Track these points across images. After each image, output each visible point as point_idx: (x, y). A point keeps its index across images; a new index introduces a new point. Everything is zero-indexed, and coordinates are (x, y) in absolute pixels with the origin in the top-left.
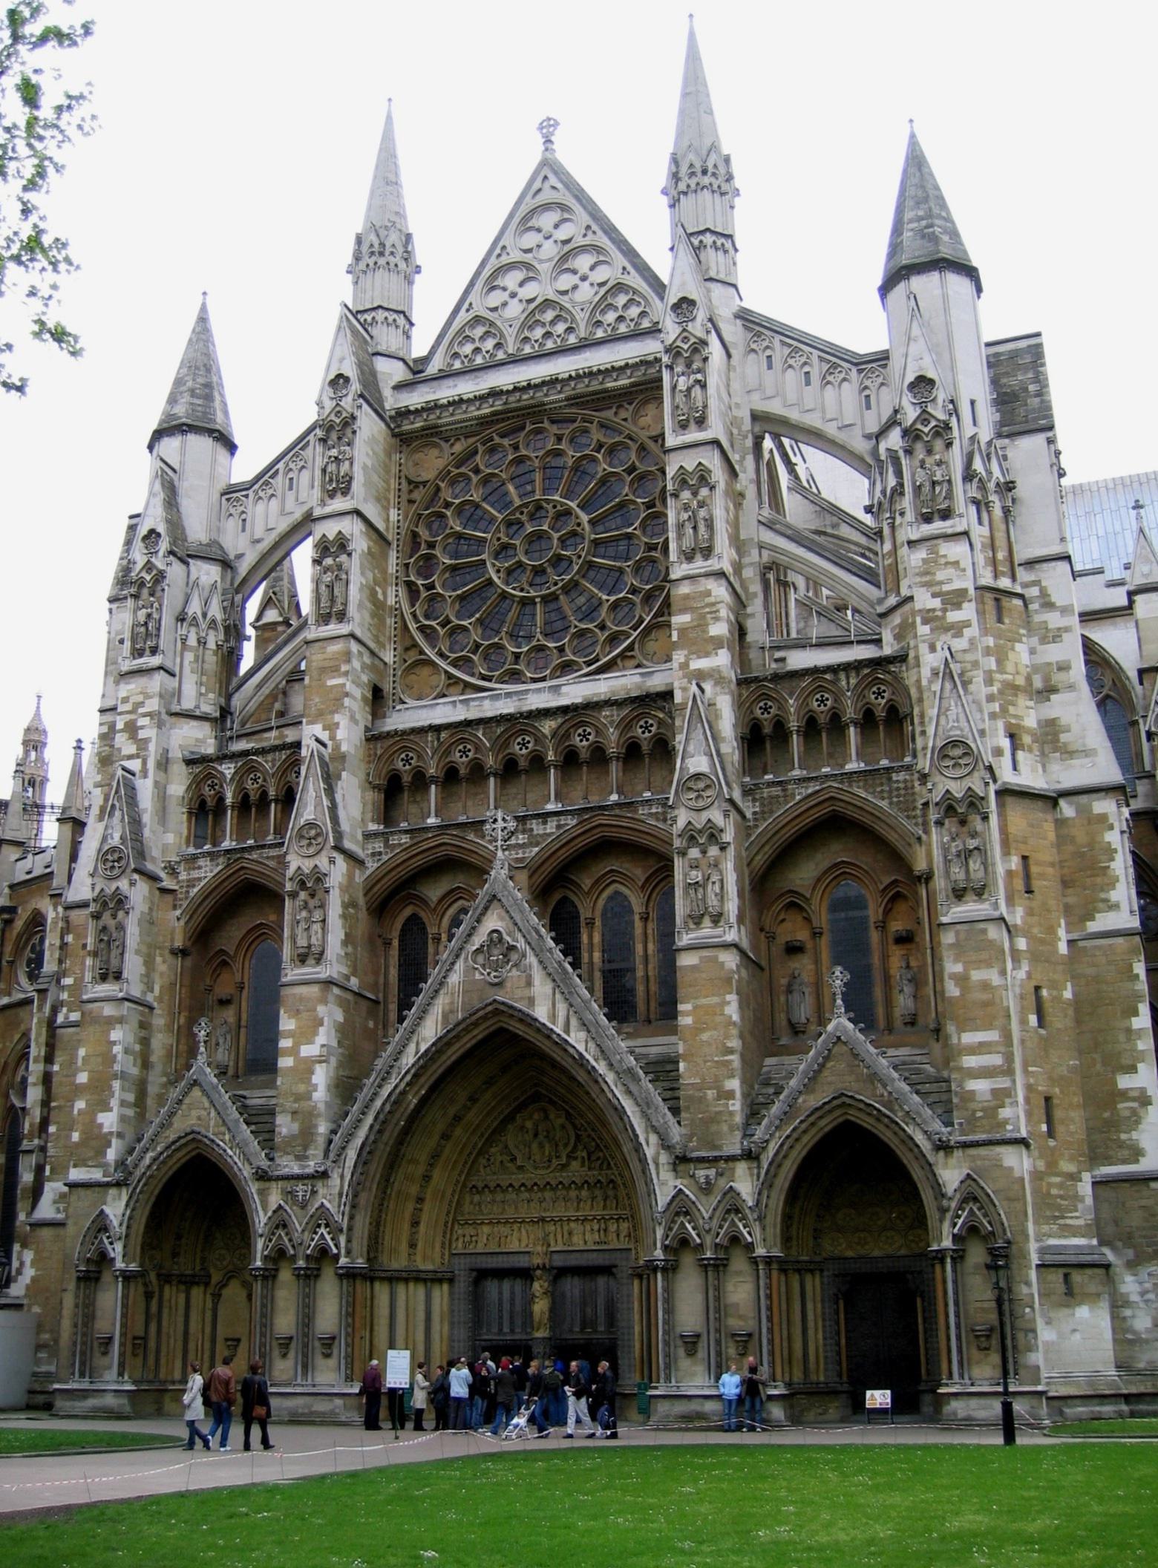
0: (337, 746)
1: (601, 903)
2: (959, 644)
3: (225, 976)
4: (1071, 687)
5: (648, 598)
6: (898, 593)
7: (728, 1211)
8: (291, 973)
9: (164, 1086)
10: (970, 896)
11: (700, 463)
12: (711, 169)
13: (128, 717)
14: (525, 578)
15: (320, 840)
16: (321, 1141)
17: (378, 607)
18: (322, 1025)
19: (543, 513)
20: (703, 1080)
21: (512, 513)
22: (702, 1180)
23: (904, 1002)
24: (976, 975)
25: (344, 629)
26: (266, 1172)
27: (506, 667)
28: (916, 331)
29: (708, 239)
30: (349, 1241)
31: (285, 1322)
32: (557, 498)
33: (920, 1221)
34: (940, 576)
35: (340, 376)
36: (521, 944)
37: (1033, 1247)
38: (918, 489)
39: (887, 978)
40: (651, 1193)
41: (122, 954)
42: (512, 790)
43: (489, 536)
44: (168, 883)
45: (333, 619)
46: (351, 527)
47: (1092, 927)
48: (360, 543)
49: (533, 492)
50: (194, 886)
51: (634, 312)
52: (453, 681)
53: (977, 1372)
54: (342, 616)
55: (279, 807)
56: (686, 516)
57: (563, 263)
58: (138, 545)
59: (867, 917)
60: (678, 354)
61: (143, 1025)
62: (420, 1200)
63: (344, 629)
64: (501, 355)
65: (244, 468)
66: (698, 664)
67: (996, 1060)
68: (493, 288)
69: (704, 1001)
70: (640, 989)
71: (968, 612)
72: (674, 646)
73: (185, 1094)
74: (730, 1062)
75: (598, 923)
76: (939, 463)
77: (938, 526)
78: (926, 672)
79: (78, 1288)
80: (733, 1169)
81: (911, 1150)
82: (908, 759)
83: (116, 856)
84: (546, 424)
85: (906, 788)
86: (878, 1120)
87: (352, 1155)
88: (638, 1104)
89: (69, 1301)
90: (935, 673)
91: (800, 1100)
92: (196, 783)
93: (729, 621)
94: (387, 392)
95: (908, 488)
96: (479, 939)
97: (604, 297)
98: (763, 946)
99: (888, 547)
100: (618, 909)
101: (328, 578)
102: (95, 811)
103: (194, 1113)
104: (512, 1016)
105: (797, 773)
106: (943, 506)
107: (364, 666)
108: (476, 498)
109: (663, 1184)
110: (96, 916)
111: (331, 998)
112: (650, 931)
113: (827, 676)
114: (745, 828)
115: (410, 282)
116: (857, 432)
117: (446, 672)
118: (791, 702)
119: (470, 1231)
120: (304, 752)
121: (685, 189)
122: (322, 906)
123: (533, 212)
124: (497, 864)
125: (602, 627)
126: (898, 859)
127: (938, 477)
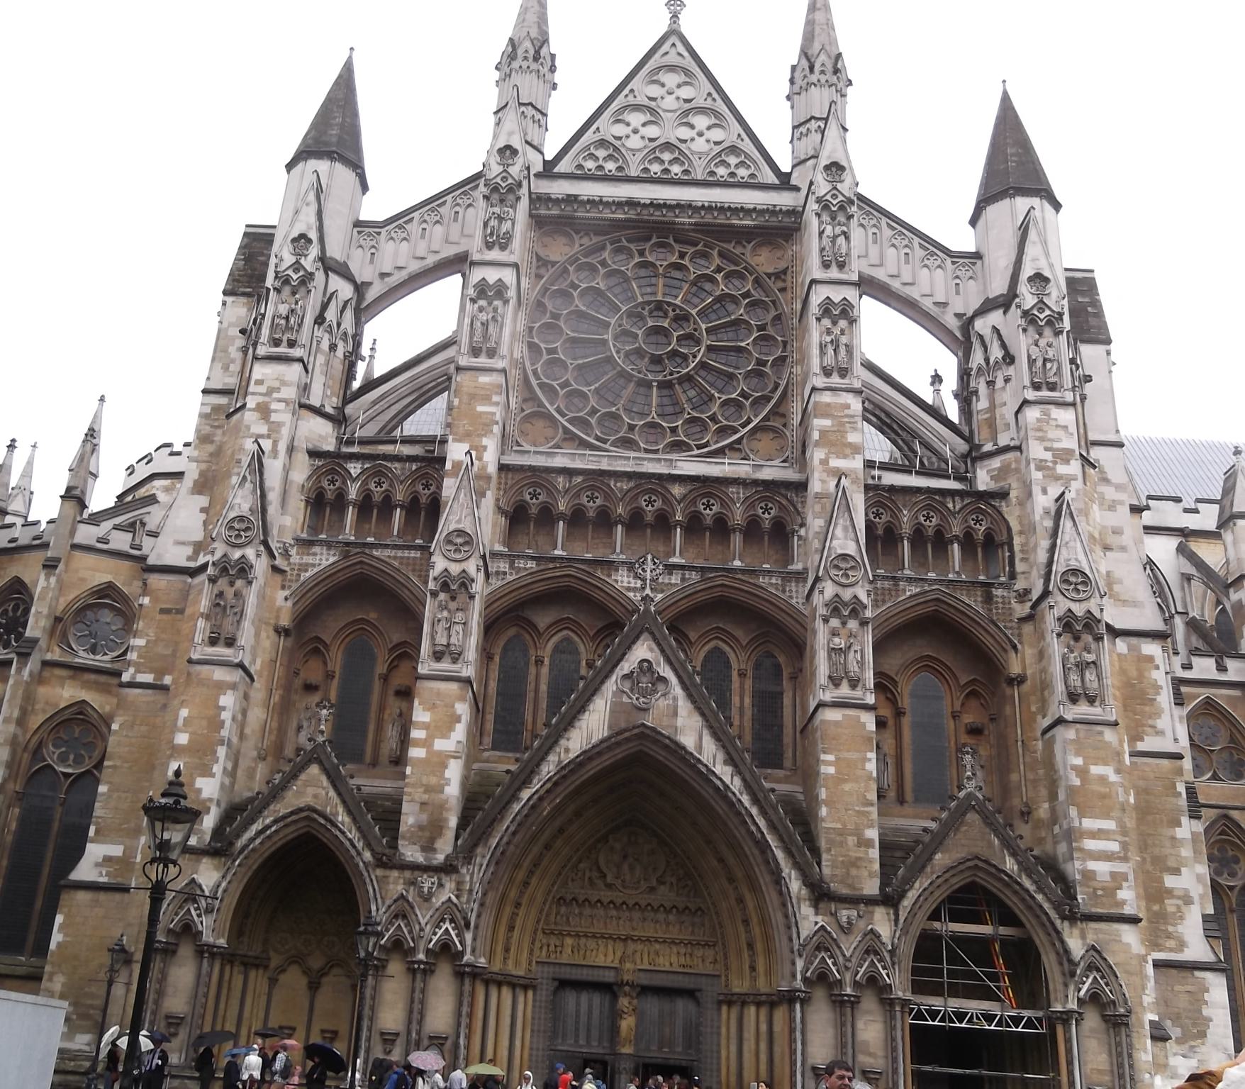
0: (484, 468)
1: (702, 655)
7: (867, 952)
8: (426, 666)
11: (845, 299)
18: (459, 721)
19: (661, 314)
22: (844, 919)
25: (500, 364)
27: (621, 434)
32: (678, 302)
35: (508, 147)
40: (790, 923)
45: (484, 354)
48: (512, 293)
49: (654, 294)
52: (570, 437)
54: (492, 353)
55: (404, 512)
56: (828, 339)
60: (826, 207)
65: (375, 208)
66: (835, 463)
68: (618, 121)
72: (817, 444)
80: (872, 913)
81: (1038, 917)
86: (1007, 885)
88: (781, 839)
91: (938, 856)
92: (316, 474)
97: (719, 154)
101: (483, 317)
104: (656, 742)
105: (907, 572)
108: (602, 286)
109: (806, 918)
112: (746, 687)
113: (937, 497)
117: (564, 427)
118: (905, 512)
120: (448, 466)
121: (815, 81)
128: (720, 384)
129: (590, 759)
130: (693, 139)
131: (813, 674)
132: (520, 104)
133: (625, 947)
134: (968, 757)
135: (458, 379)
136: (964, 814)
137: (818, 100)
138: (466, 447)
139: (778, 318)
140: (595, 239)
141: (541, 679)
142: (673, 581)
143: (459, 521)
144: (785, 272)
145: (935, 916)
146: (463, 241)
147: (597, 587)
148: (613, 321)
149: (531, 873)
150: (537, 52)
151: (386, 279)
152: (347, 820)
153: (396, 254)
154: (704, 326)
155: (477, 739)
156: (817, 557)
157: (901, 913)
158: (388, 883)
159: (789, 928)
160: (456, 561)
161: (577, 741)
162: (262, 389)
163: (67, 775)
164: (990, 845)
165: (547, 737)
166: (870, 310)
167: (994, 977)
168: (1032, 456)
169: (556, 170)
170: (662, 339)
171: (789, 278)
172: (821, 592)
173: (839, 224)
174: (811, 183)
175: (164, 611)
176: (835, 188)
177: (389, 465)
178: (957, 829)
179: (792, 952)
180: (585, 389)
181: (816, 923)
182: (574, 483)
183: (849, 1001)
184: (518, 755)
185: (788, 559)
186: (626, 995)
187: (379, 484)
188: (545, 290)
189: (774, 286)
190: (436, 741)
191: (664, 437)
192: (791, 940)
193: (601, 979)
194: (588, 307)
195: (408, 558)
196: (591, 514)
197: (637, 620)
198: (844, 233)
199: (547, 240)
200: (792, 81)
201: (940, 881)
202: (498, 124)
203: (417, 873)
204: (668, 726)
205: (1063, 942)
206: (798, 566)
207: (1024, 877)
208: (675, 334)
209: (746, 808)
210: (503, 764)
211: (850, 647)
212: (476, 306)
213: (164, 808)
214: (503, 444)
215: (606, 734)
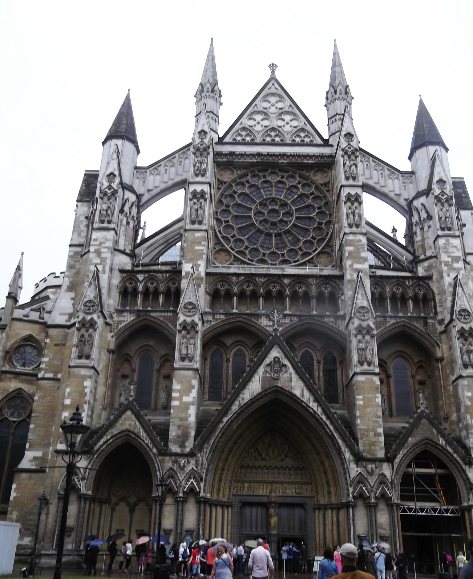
0: (200, 274)
3: (126, 365)
6: (425, 255)
7: (381, 483)
9: (101, 410)
14: (268, 226)
15: (193, 310)
16: (192, 439)
18: (193, 387)
19: (274, 203)
20: (368, 428)
21: (263, 200)
22: (370, 469)
25: (205, 227)
26: (165, 451)
27: (260, 257)
30: (205, 486)
31: (168, 523)
32: (282, 198)
34: (451, 250)
35: (203, 131)
38: (440, 218)
40: (346, 472)
41: (91, 348)
43: (253, 207)
44: (108, 320)
49: (271, 194)
50: (121, 324)
52: (236, 260)
54: (200, 223)
56: (350, 211)
60: (346, 153)
61: (96, 382)
65: (143, 161)
66: (356, 266)
68: (250, 119)
69: (367, 395)
72: (348, 258)
73: (124, 412)
74: (379, 421)
76: (447, 211)
77: (446, 232)
78: (446, 284)
79: (59, 503)
80: (382, 465)
81: (455, 464)
83: (91, 304)
84: (277, 171)
85: (432, 325)
86: (441, 450)
90: (450, 284)
91: (410, 439)
92: (123, 280)
97: (296, 132)
101: (196, 207)
103: (127, 422)
105: (390, 314)
106: (449, 226)
108: (248, 192)
109: (353, 469)
112: (321, 368)
117: (234, 255)
118: (387, 287)
120: (183, 274)
123: (268, 95)
127: (448, 214)
128: (302, 233)
129: (254, 402)
130: (284, 126)
131: (351, 360)
132: (208, 112)
133: (272, 486)
134: (421, 395)
135: (186, 235)
136: (421, 420)
137: (339, 106)
138: (191, 265)
139: (326, 204)
140: (243, 171)
141: (229, 368)
142: (286, 322)
143: (190, 298)
144: (328, 183)
145: (409, 466)
146: (184, 174)
147: (253, 326)
148: (253, 207)
149: (228, 455)
151: (151, 192)
152: (145, 435)
153: (154, 181)
154: (294, 208)
156: (350, 308)
157: (395, 465)
158: (165, 463)
159: (345, 474)
160: (189, 316)
161: (247, 395)
162: (97, 243)
163: (14, 422)
164: (433, 433)
165: (234, 394)
166: (366, 197)
167: (436, 492)
168: (442, 260)
169: (224, 141)
170: (275, 215)
171: (330, 186)
172: (353, 323)
173: (352, 160)
174: (339, 142)
175: (56, 345)
176: (349, 144)
177: (156, 275)
178: (418, 427)
179: (347, 484)
180: (242, 238)
181: (357, 471)
182: (240, 279)
183: (373, 505)
184: (220, 402)
185: (337, 310)
186: (273, 507)
187: (152, 284)
188: (222, 195)
189: (324, 189)
191: (279, 258)
192: (346, 479)
193: (261, 501)
194: (242, 201)
195: (167, 316)
196: (248, 293)
197: (271, 339)
198: (355, 164)
199: (222, 172)
200: (327, 98)
201: (411, 450)
202: (197, 121)
203: (177, 457)
204: (288, 386)
205: (466, 475)
206: (341, 313)
207: (448, 447)
208: (281, 212)
209: (324, 422)
210: (214, 407)
211: (367, 348)
212: (192, 202)
213: (71, 426)
214: (207, 263)
215: (260, 391)
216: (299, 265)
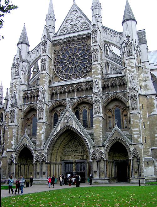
1: (82, 111)
2: (133, 74)
3: (29, 122)
4: (149, 80)
5: (89, 67)
8: (38, 121)
10: (135, 109)
12: (98, 5)
13: (14, 85)
16: (43, 145)
17: (50, 68)
23: (125, 124)
24: (135, 121)
25: (45, 72)
28: (127, 29)
29: (98, 16)
31: (38, 170)
33: (127, 155)
36: (71, 117)
37: (143, 158)
38: (127, 52)
39: (123, 121)
40: (90, 151)
42: (69, 95)
44: (20, 108)
46: (47, 57)
47: (152, 114)
48: (48, 60)
51: (87, 26)
53: (135, 176)
54: (45, 70)
57: (77, 19)
58: (15, 60)
59: (120, 113)
61: (17, 129)
62: (57, 153)
63: (45, 72)
64: (68, 32)
65: (31, 49)
66: (96, 77)
67: (138, 132)
70: (88, 123)
71: (134, 69)
72: (93, 74)
75: (82, 113)
77: (130, 57)
78: (128, 78)
82: (126, 90)
84: (74, 42)
87: (47, 147)
89: (7, 168)
92: (24, 94)
93: (100, 70)
94: (51, 38)
95: (126, 52)
96: (65, 116)
98: (106, 117)
99: (123, 60)
100: (85, 111)
101: (43, 65)
102: (10, 98)
105: (110, 92)
107: (48, 77)
109: (91, 150)
110: (10, 113)
111: (44, 125)
114: (103, 100)
115: (55, 22)
116: (119, 43)
119: (64, 157)
122: (43, 112)
124: (67, 105)
125: (82, 71)
126: (124, 104)
137: (97, 11)
150: (50, 16)
154: (80, 56)
155: (51, 129)
190: (40, 132)
216: (82, 78)
